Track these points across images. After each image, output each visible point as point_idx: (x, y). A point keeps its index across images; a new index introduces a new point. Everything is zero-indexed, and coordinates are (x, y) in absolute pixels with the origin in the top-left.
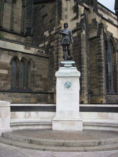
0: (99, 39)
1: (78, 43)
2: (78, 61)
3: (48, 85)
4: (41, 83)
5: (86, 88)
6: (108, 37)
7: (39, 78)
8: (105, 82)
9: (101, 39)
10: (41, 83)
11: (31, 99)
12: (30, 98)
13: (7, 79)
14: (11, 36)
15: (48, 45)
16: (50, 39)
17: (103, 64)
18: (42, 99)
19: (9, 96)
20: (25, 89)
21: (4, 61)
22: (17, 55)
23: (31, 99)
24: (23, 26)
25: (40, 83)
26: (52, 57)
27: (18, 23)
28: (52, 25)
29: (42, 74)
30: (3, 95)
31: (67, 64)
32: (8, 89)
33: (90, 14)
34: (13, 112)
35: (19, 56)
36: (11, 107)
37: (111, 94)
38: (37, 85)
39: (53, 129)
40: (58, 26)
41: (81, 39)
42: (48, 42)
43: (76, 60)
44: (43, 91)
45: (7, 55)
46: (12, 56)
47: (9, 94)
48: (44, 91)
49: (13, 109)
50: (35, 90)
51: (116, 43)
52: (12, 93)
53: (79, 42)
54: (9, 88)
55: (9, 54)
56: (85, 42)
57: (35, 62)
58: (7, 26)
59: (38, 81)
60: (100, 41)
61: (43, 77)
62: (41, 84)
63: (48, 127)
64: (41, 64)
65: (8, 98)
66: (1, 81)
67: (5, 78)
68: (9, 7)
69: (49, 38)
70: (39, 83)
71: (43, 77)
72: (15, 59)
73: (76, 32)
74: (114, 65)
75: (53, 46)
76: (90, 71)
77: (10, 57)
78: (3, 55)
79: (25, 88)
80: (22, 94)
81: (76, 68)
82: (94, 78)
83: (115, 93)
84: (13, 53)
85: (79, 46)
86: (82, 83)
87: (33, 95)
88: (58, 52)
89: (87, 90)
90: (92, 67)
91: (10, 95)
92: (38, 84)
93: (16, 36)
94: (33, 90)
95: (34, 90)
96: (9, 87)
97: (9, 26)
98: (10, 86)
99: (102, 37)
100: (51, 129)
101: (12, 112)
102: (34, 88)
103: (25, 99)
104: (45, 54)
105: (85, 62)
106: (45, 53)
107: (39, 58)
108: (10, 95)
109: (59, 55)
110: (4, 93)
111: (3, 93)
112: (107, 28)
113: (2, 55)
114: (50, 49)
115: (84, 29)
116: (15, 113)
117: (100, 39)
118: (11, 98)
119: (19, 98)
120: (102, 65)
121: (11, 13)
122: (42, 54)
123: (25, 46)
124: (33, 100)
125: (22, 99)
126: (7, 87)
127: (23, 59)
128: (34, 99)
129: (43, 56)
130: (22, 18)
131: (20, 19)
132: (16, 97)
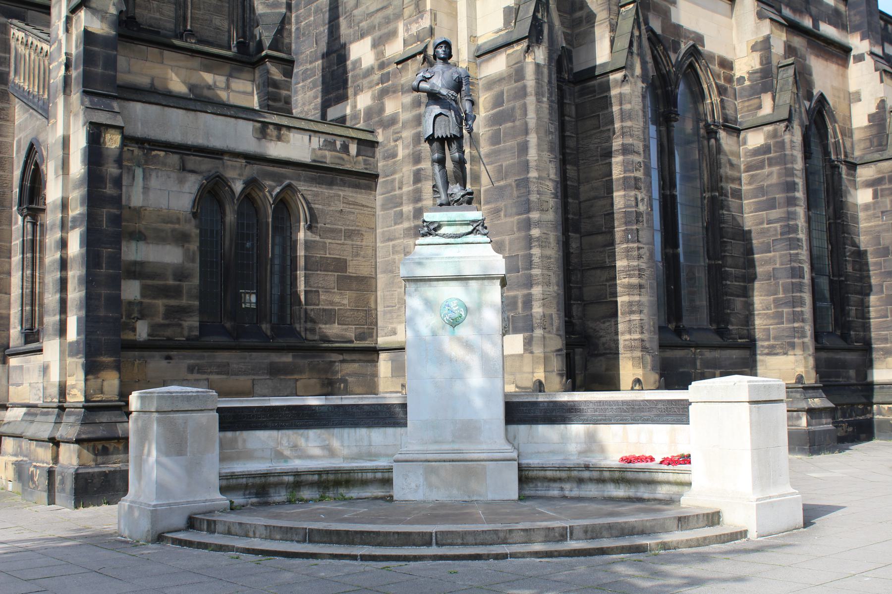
1: (511, 105)
2: (515, 193)
3: (376, 309)
4: (346, 302)
5: (552, 319)
6: (673, 57)
7: (331, 278)
8: (651, 288)
10: (346, 302)
11: (297, 380)
12: (292, 372)
13: (179, 286)
14: (181, 64)
15: (369, 113)
16: (382, 81)
17: (642, 199)
18: (350, 379)
19: (191, 369)
20: (269, 333)
21: (163, 204)
22: (221, 170)
23: (297, 380)
24: (240, 11)
25: (337, 299)
26: (393, 173)
28: (389, 11)
29: (349, 258)
30: (164, 363)
31: (451, 223)
32: (186, 333)
34: (229, 434)
35: (230, 174)
36: (219, 410)
37: (697, 347)
38: (324, 310)
40: (416, 21)
41: (524, 87)
42: (373, 98)
43: (505, 186)
44: (352, 342)
45: (174, 175)
46: (200, 178)
48: (361, 337)
49: (232, 421)
50: (317, 337)
51: (722, 82)
52: (206, 354)
53: (518, 104)
54: (191, 328)
55: (183, 168)
56: (545, 99)
57: (309, 198)
58: (157, 15)
59: (327, 291)
61: (351, 271)
63: (379, 492)
64: (341, 206)
65: (190, 377)
66: (154, 298)
67: (171, 282)
69: (376, 76)
71: (351, 271)
72: (212, 193)
73: (501, 53)
74: (713, 199)
75: (393, 121)
76: (578, 235)
78: (157, 177)
79: (265, 327)
80: (254, 354)
81: (488, 240)
82: (598, 271)
83: (716, 340)
84: (207, 165)
85: (517, 123)
86: (534, 297)
87: (307, 361)
88: (420, 154)
89: (558, 330)
90: (589, 217)
91: (198, 362)
92: (331, 307)
93: (206, 62)
94: (303, 334)
95: (310, 337)
96: (192, 323)
97: (172, 14)
98: (197, 319)
100: (390, 499)
101: (222, 434)
102: (309, 325)
103: (269, 382)
104: (360, 158)
105: (547, 199)
106: (358, 154)
107: (329, 176)
108: (197, 365)
109: (422, 165)
110: (172, 353)
111: (166, 353)
112: (673, 9)
113: (154, 174)
114: (380, 131)
115: (539, 42)
116: (234, 441)
119: (242, 378)
120: (637, 205)
122: (344, 156)
123: (258, 125)
125: (253, 380)
126: (180, 325)
127: (252, 183)
128: (313, 381)
129: (348, 167)
132: (224, 369)
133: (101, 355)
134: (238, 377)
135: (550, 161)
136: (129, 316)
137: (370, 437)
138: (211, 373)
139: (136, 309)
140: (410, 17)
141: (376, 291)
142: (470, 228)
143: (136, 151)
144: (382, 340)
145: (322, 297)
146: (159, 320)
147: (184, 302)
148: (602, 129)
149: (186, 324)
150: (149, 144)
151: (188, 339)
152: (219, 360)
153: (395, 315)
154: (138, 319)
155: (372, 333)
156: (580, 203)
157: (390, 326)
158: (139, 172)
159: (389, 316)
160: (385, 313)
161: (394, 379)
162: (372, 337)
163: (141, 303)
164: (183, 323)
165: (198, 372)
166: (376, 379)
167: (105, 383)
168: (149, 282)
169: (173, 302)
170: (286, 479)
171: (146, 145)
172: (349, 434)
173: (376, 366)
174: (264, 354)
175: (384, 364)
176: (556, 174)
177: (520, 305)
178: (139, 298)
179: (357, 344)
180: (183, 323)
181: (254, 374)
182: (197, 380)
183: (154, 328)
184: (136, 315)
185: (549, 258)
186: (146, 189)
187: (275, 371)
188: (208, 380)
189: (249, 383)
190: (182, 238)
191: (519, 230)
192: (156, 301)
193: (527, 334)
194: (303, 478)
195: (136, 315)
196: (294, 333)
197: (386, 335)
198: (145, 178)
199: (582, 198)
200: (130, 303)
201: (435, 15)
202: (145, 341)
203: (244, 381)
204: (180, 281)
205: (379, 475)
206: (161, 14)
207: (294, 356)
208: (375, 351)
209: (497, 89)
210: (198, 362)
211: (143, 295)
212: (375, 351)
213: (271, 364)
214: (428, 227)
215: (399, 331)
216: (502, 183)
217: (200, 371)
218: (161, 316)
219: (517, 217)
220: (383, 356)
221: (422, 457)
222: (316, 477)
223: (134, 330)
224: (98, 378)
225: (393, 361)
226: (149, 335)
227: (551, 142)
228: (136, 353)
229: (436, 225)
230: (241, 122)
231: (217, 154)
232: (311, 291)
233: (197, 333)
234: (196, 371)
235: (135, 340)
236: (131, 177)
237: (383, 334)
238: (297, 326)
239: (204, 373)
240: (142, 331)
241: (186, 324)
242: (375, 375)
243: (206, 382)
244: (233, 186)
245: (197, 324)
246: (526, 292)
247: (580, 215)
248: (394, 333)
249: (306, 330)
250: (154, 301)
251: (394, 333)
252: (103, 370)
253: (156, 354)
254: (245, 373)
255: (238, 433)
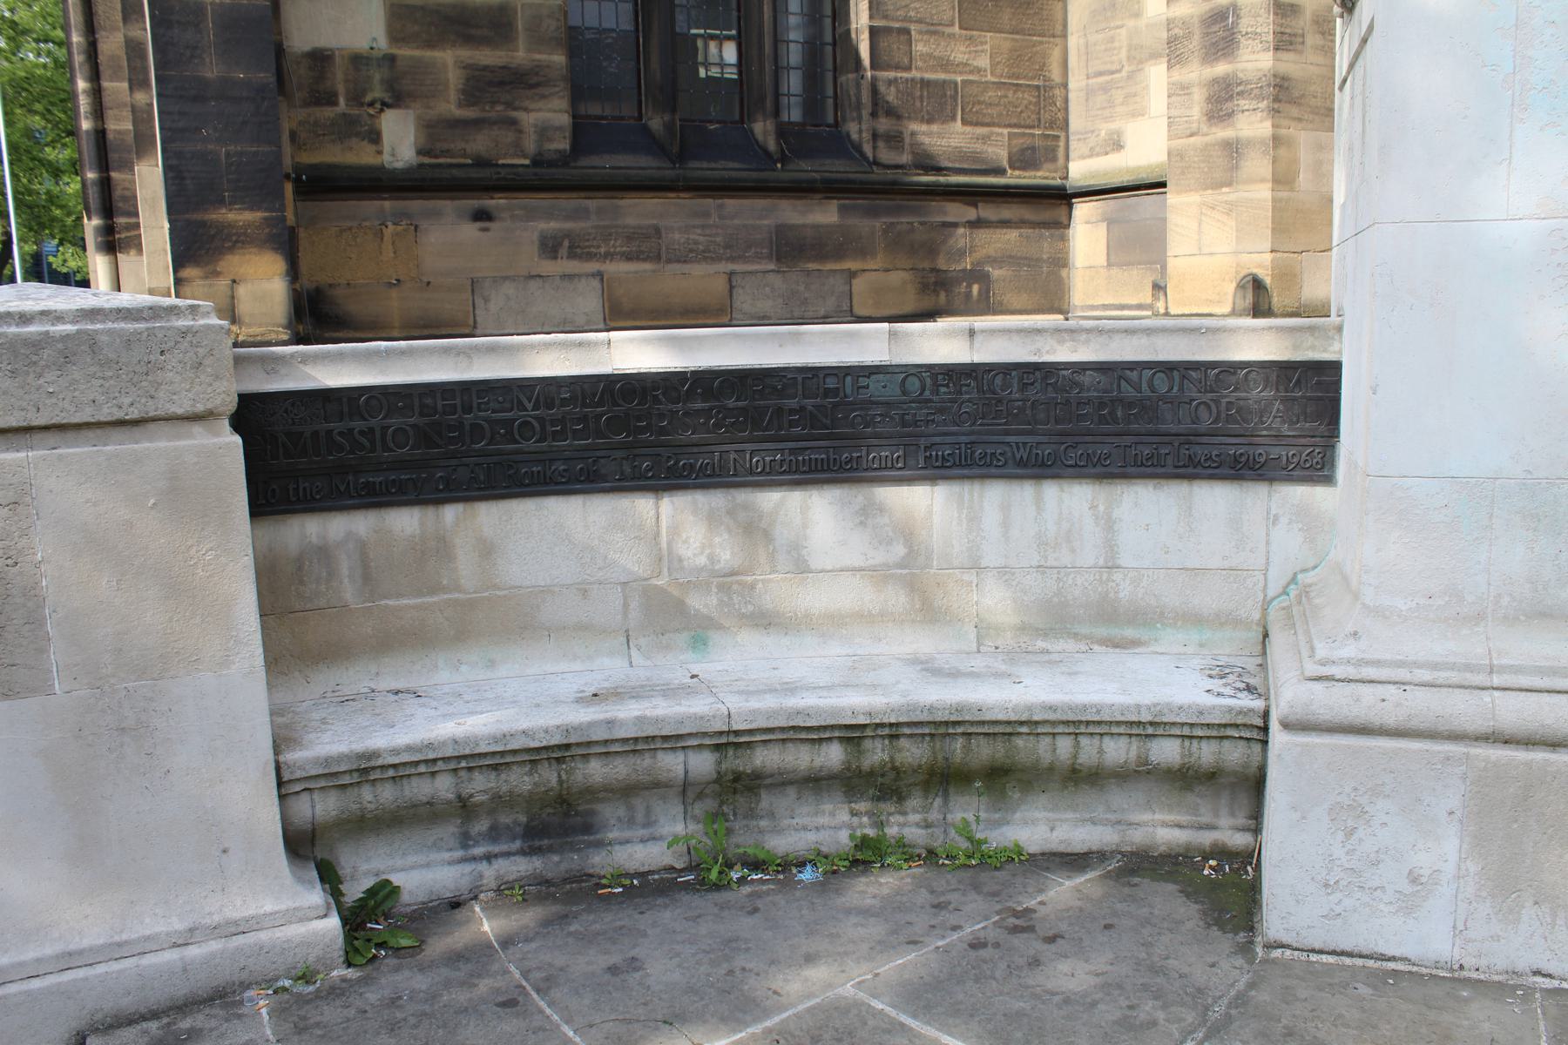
3: (1065, 86)
4: (983, 62)
10: (983, 62)
11: (852, 274)
12: (839, 254)
18: (996, 273)
19: (550, 247)
20: (772, 145)
23: (852, 274)
25: (959, 53)
30: (470, 230)
32: (530, 145)
38: (925, 84)
39: (1292, 904)
44: (1000, 171)
47: (550, 216)
48: (1025, 158)
50: (905, 158)
52: (592, 204)
54: (544, 132)
59: (934, 30)
62: (979, 70)
63: (1162, 826)
66: (430, 45)
70: (945, 65)
79: (762, 129)
80: (731, 204)
87: (878, 224)
91: (569, 225)
92: (942, 76)
94: (868, 149)
95: (886, 156)
96: (547, 117)
102: (884, 124)
103: (777, 280)
108: (567, 234)
118: (593, 266)
119: (698, 270)
124: (877, 275)
125: (731, 274)
126: (513, 122)
128: (896, 278)
132: (647, 245)
133: (221, 202)
134: (686, 268)
136: (356, 98)
137: (1109, 525)
138: (609, 256)
139: (377, 77)
141: (1065, 36)
144: (1081, 170)
145: (919, 48)
146: (450, 106)
147: (521, 55)
149: (529, 119)
151: (537, 162)
152: (631, 221)
153: (1118, 95)
154: (385, 105)
155: (1054, 150)
157: (1104, 128)
159: (1100, 99)
160: (1089, 93)
161: (1115, 271)
162: (1054, 159)
163: (391, 59)
164: (521, 115)
165: (572, 255)
166: (1064, 273)
167: (242, 291)
169: (488, 57)
170: (672, 764)
172: (1005, 508)
173: (1064, 239)
174: (760, 203)
175: (1087, 231)
178: (383, 44)
179: (1014, 178)
180: (521, 115)
181: (732, 259)
182: (569, 277)
183: (434, 132)
184: (377, 93)
187: (790, 249)
188: (600, 275)
189: (720, 285)
192: (437, 54)
194: (766, 758)
195: (377, 93)
196: (841, 145)
197: (1092, 154)
200: (358, 60)
202: (408, 170)
203: (704, 278)
205: (1167, 752)
207: (842, 210)
208: (1062, 197)
210: (569, 225)
211: (395, 37)
212: (1062, 197)
213: (781, 230)
215: (1129, 139)
217: (577, 248)
218: (453, 96)
220: (1083, 210)
221: (1465, 709)
222: (833, 756)
223: (375, 137)
224: (216, 274)
225: (1111, 222)
226: (420, 152)
228: (387, 204)
232: (888, 30)
233: (563, 144)
234: (563, 251)
235: (382, 168)
237: (1086, 151)
238: (852, 129)
239: (590, 257)
240: (399, 140)
241: (529, 119)
242: (1061, 261)
243: (596, 283)
245: (565, 119)
248: (1116, 145)
249: (875, 136)
250: (428, 54)
251: (1116, 145)
252: (231, 249)
253: (447, 206)
254: (707, 256)
255: (450, 513)
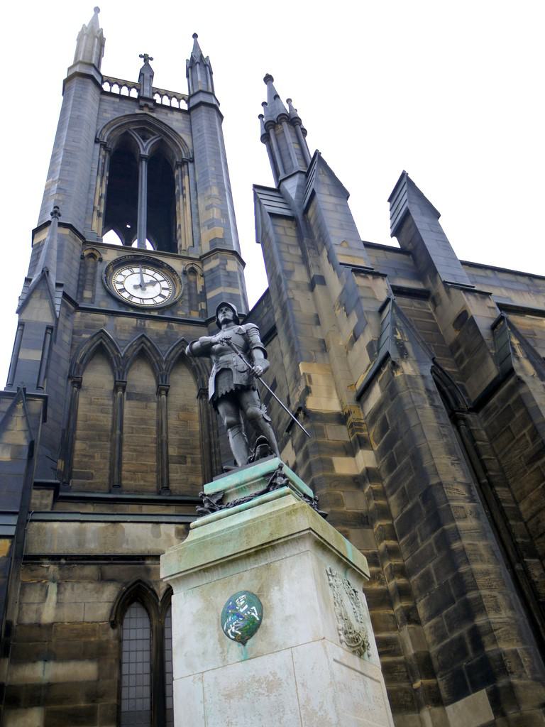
0: (511, 381)
5: (518, 656)
9: (524, 378)
22: (143, 576)
27: (189, 460)
31: (241, 487)
33: (439, 308)
58: (142, 483)
60: (522, 391)
67: (82, 704)
68: (145, 410)
73: (374, 384)
77: (110, 593)
89: (533, 671)
97: (155, 480)
99: (522, 368)
117: (520, 382)
121: (155, 432)
130: (202, 440)
131: (198, 443)
135: (452, 464)
140: (293, 390)
142: (263, 487)
143: (52, 568)
148: (517, 438)
150: (66, 560)
156: (526, 523)
158: (53, 588)
168: (56, 707)
171: (63, 561)
176: (464, 476)
177: (469, 647)
185: (487, 573)
186: (59, 603)
190: (96, 653)
191: (439, 549)
193: (490, 687)
198: (59, 593)
199: (526, 516)
201: (310, 377)
204: (93, 701)
206: (145, 481)
209: (380, 418)
214: (209, 501)
216: (409, 506)
219: (433, 536)
227: (447, 444)
229: (220, 497)
230: (162, 526)
231: (138, 560)
236: (43, 593)
244: (155, 589)
246: (467, 627)
247: (531, 537)
